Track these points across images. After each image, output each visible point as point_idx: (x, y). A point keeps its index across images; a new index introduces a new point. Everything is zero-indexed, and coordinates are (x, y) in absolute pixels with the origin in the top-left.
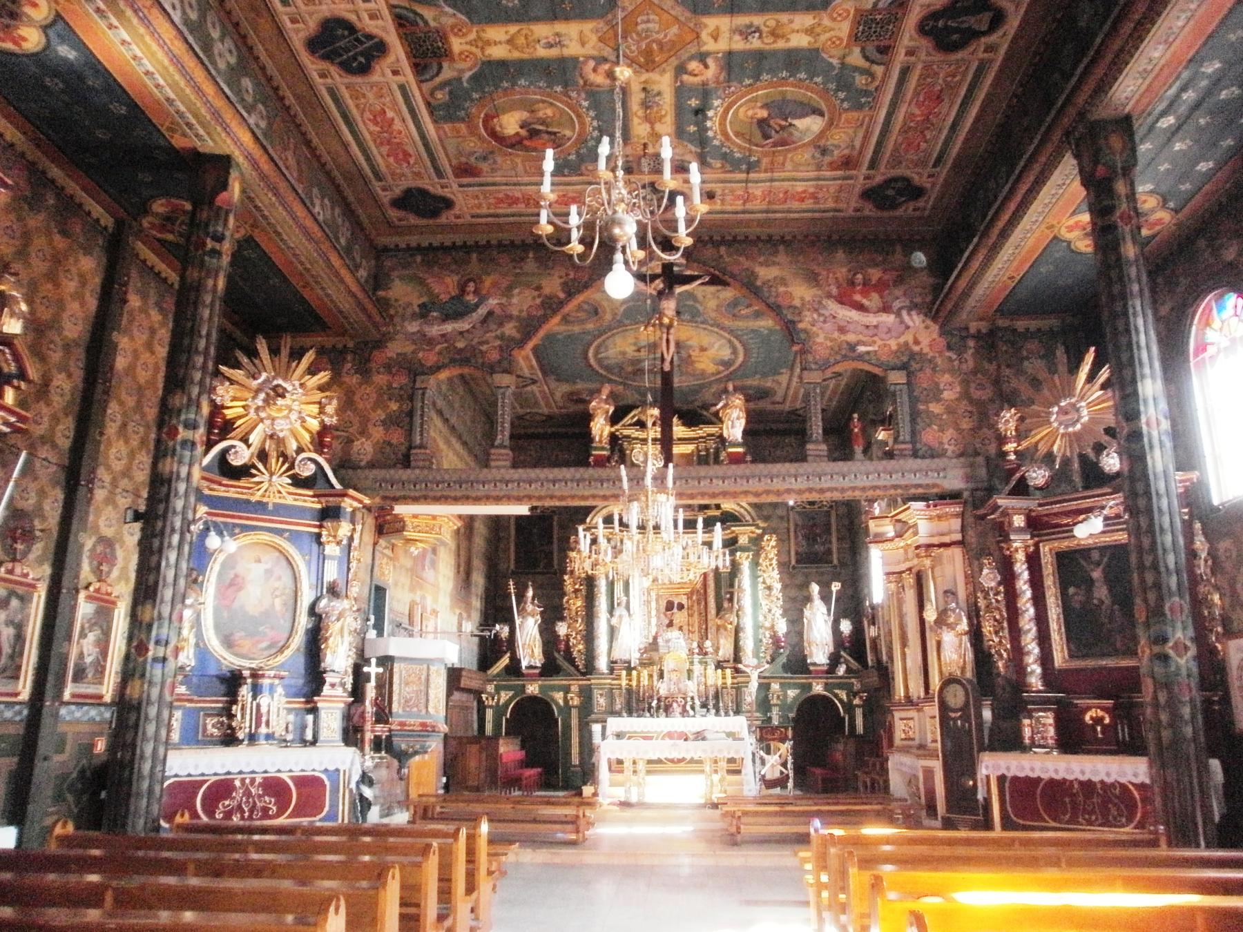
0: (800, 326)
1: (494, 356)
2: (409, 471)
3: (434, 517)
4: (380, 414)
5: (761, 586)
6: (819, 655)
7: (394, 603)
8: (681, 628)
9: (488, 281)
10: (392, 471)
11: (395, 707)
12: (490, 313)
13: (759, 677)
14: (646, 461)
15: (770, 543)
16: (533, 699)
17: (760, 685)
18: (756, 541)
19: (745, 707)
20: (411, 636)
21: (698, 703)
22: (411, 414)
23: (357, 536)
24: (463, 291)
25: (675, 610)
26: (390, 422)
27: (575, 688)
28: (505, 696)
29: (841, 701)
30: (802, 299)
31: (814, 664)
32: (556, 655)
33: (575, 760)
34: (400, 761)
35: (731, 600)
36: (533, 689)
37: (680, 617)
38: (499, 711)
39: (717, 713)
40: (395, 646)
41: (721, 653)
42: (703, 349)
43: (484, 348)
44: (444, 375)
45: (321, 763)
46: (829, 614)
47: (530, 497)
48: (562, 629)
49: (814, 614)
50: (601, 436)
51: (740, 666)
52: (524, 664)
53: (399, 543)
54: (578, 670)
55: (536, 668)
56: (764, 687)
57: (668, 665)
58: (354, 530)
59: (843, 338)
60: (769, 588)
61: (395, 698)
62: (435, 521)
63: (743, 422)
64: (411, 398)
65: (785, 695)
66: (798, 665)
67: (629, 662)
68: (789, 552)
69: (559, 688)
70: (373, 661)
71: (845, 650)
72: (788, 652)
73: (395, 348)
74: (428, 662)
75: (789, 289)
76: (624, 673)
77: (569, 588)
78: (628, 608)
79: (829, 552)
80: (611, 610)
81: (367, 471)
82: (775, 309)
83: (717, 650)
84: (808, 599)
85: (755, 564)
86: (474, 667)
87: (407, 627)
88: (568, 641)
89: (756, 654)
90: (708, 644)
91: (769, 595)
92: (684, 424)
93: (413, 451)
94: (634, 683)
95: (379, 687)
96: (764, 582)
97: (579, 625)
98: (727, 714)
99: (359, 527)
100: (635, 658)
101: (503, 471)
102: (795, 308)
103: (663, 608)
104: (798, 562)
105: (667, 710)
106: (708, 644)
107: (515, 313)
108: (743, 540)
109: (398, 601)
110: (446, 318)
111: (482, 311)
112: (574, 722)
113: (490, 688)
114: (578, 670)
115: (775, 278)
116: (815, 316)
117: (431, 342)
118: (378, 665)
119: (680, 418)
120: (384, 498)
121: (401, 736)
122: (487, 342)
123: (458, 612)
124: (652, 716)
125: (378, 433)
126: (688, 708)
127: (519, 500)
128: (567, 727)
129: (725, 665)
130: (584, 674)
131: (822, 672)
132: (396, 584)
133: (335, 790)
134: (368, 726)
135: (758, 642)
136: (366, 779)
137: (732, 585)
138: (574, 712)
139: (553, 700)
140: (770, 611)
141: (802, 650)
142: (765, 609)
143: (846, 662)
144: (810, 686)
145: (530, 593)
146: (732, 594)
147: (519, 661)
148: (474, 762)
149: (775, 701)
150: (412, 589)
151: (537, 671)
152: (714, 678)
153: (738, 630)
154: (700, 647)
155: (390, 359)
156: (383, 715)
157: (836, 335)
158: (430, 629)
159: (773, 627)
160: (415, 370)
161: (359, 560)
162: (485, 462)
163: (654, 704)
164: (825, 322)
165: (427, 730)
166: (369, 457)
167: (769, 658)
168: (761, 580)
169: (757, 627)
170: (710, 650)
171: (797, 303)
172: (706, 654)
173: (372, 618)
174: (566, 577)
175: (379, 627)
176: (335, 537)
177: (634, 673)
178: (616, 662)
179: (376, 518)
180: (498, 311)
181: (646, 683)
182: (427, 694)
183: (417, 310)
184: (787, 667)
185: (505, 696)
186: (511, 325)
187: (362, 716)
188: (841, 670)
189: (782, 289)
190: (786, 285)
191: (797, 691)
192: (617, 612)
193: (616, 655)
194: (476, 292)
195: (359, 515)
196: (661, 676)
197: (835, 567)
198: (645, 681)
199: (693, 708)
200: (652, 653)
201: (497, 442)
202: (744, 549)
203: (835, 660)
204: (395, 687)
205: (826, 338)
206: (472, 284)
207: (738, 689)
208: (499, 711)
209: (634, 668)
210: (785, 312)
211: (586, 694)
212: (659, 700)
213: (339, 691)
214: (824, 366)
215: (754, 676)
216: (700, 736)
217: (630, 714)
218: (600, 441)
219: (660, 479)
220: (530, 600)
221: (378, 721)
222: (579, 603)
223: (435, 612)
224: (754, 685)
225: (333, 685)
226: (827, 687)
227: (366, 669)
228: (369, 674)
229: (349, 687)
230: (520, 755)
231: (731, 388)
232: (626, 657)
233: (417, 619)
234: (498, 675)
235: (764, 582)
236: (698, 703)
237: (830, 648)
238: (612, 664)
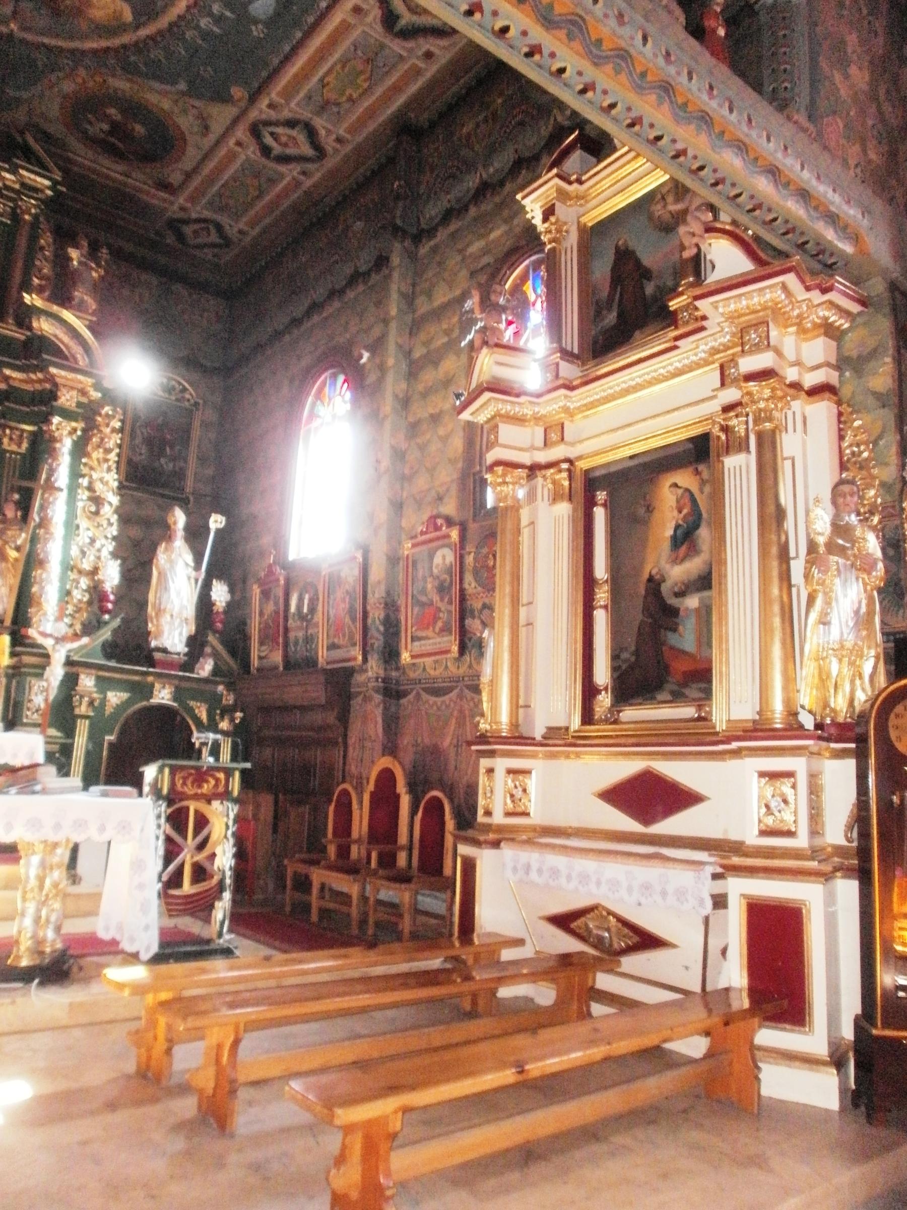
5: (83, 495)
6: (172, 632)
19: (29, 716)
31: (165, 651)
35: (25, 506)
46: (197, 567)
49: (171, 562)
56: (70, 681)
60: (97, 501)
65: (104, 700)
66: (131, 647)
71: (215, 632)
72: (117, 622)
79: (180, 475)
84: (167, 533)
85: (80, 450)
91: (97, 513)
108: (67, 399)
131: (171, 665)
140: (93, 541)
143: (215, 655)
144: (147, 691)
149: (83, 709)
153: (32, 562)
159: (95, 571)
168: (85, 482)
169: (68, 567)
184: (111, 650)
188: (206, 668)
191: (125, 696)
202: (67, 415)
224: (56, 673)
226: (178, 695)
235: (90, 488)
237: (191, 628)
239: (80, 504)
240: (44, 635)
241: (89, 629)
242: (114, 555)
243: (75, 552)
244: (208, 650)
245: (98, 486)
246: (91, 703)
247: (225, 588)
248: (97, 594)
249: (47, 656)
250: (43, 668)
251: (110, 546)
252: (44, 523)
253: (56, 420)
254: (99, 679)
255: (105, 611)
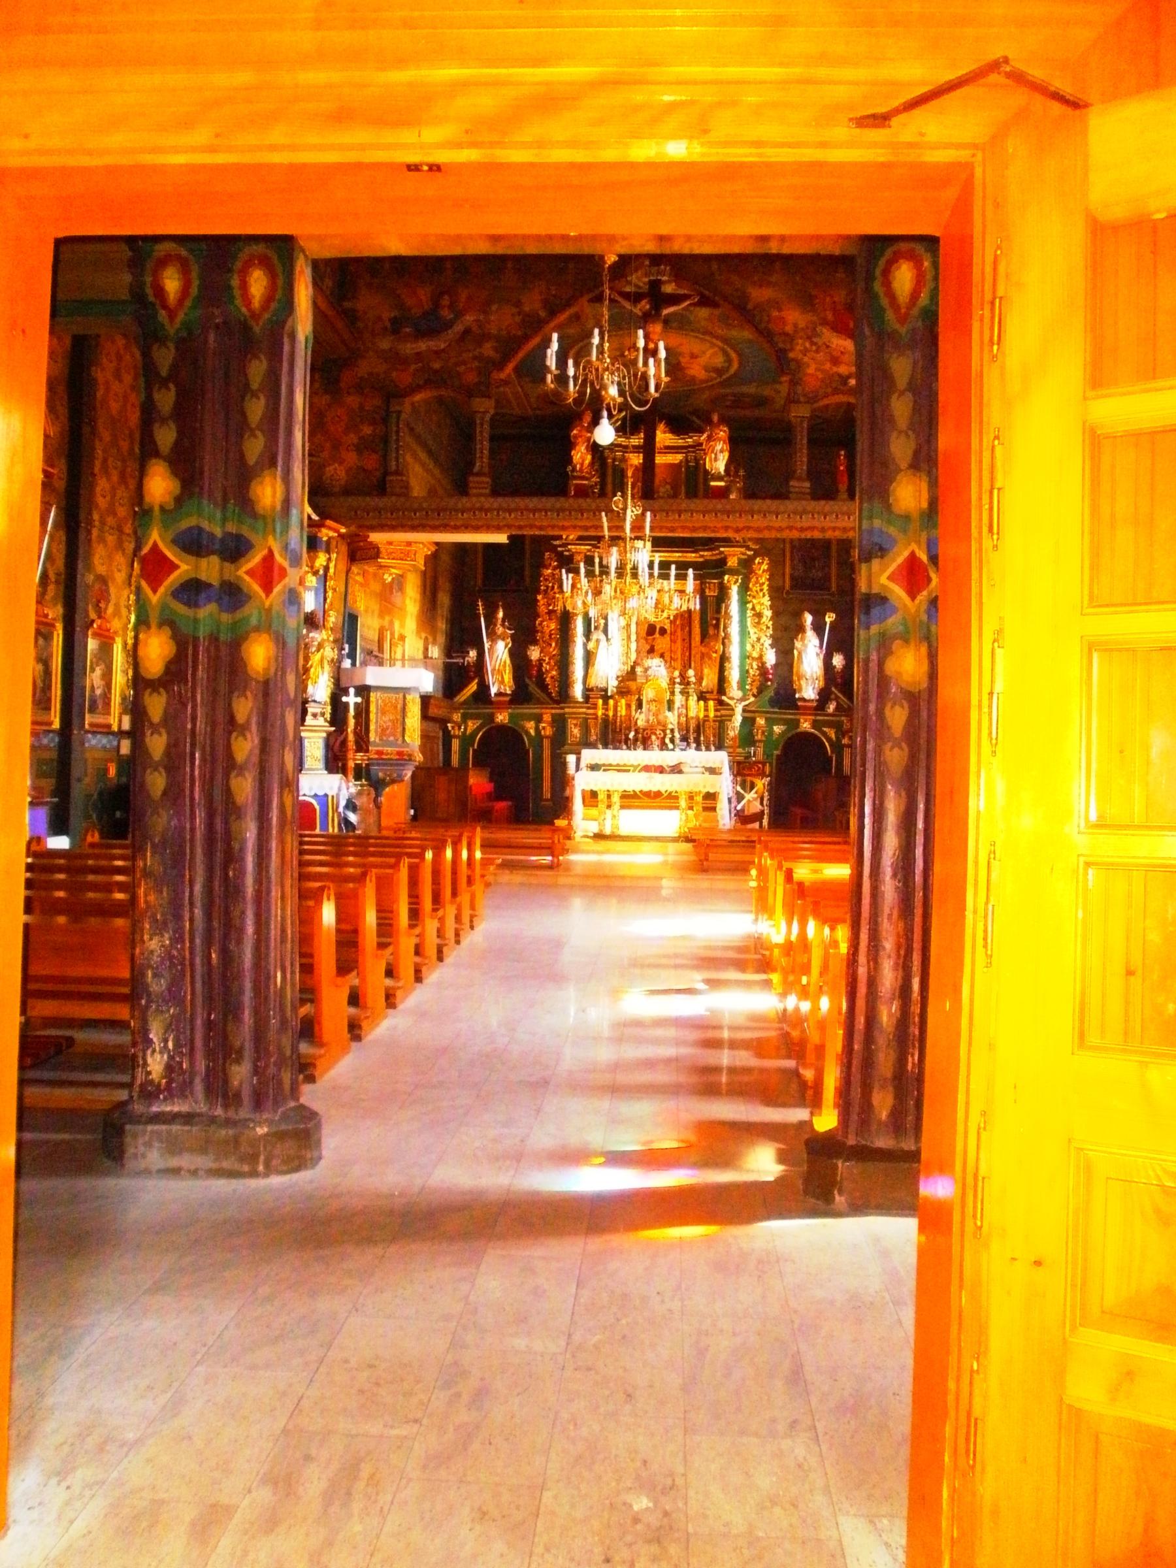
0: (791, 355)
1: (471, 378)
2: (385, 499)
3: (409, 544)
4: (353, 438)
5: (749, 613)
7: (366, 630)
8: (662, 656)
9: (463, 295)
10: (368, 499)
11: (373, 737)
12: (467, 331)
13: (744, 711)
14: (625, 509)
15: (762, 566)
16: (502, 728)
17: (745, 719)
18: (747, 566)
19: (728, 742)
20: (381, 664)
21: (677, 735)
22: (385, 440)
23: (332, 565)
24: (437, 305)
25: (657, 635)
26: (362, 447)
27: (547, 717)
28: (472, 725)
29: (829, 739)
30: (795, 325)
31: (803, 700)
32: (527, 680)
33: (547, 794)
34: (376, 790)
35: (717, 626)
36: (502, 717)
37: (662, 643)
38: (466, 741)
39: (698, 748)
40: (373, 676)
41: (704, 683)
42: (693, 356)
43: (462, 369)
44: (418, 397)
45: (311, 789)
46: (821, 647)
47: (509, 527)
48: (534, 653)
49: (805, 646)
50: (582, 465)
51: (724, 698)
52: (494, 690)
53: (371, 569)
54: (552, 698)
55: (505, 695)
56: (749, 722)
57: (648, 694)
58: (329, 560)
59: (835, 369)
61: (372, 727)
62: (408, 549)
63: (727, 455)
64: (385, 421)
65: (771, 732)
67: (606, 690)
68: (784, 574)
69: (530, 717)
70: (352, 691)
73: (364, 368)
74: (405, 691)
75: (784, 314)
76: (600, 702)
77: (542, 609)
78: (605, 631)
79: (827, 578)
80: (588, 634)
81: (342, 499)
82: (767, 334)
83: (700, 679)
84: (801, 629)
85: (744, 589)
86: (440, 695)
87: (376, 657)
88: (541, 665)
89: (741, 685)
90: (691, 673)
91: (759, 623)
92: (673, 431)
93: (389, 478)
94: (611, 713)
95: (357, 716)
96: (753, 609)
97: (553, 649)
98: (708, 749)
99: (334, 556)
100: (612, 685)
101: (483, 499)
102: (787, 335)
103: (643, 633)
104: (792, 588)
105: (646, 743)
106: (691, 673)
107: (494, 331)
108: (732, 562)
109: (369, 628)
110: (420, 334)
111: (459, 328)
112: (547, 753)
113: (457, 717)
114: (552, 698)
115: (769, 301)
116: (807, 345)
117: (404, 361)
118: (357, 695)
119: (667, 424)
120: (360, 527)
121: (378, 765)
122: (464, 363)
123: (423, 635)
124: (629, 748)
125: (351, 458)
126: (667, 741)
127: (498, 529)
128: (539, 758)
129: (708, 696)
130: (558, 702)
132: (366, 611)
133: (325, 814)
134: (350, 755)
135: (744, 673)
136: (351, 805)
137: (718, 611)
138: (546, 743)
139: (523, 727)
140: (759, 639)
141: (791, 682)
142: (754, 637)
143: (837, 699)
145: (501, 614)
146: (718, 620)
147: (488, 688)
148: (442, 792)
150: (381, 615)
151: (507, 699)
152: (696, 709)
154: (683, 676)
155: (361, 378)
156: (362, 743)
157: (828, 366)
158: (399, 656)
159: (761, 657)
160: (392, 394)
161: (334, 590)
162: (462, 488)
163: (632, 735)
164: (817, 351)
165: (403, 758)
166: (343, 482)
167: (755, 691)
168: (750, 606)
169: (744, 656)
170: (693, 679)
171: (789, 329)
172: (688, 683)
173: (347, 646)
174: (539, 597)
175: (352, 655)
176: (312, 567)
177: (611, 702)
178: (591, 690)
179: (349, 544)
180: (475, 328)
181: (624, 713)
182: (404, 723)
183: (388, 324)
184: (773, 702)
185: (472, 725)
186: (488, 345)
187: (344, 743)
188: (831, 707)
189: (775, 313)
190: (780, 310)
191: (783, 728)
192: (594, 637)
193: (592, 682)
194: (451, 307)
195: (334, 543)
196: (640, 705)
197: (833, 595)
198: (622, 711)
199: (672, 741)
200: (629, 682)
201: (476, 469)
202: (732, 572)
203: (824, 695)
204: (372, 716)
205: (817, 369)
206: (446, 297)
207: (722, 723)
208: (466, 741)
209: (612, 697)
210: (775, 339)
211: (560, 723)
212: (637, 732)
213: (321, 721)
214: (812, 399)
215: (739, 710)
216: (677, 769)
217: (606, 746)
218: (581, 470)
219: (638, 526)
220: (500, 621)
221: (359, 750)
222: (553, 626)
223: (402, 638)
224: (738, 719)
225: (315, 715)
226: (815, 724)
227: (344, 699)
228: (347, 705)
229: (328, 716)
230: (490, 787)
231: (715, 418)
232: (602, 685)
233: (387, 646)
234: (465, 703)
235: (753, 609)
236: (677, 735)
237: (821, 683)
238: (588, 691)
239: (749, 620)
240: (732, 699)
241: (761, 690)
242: (772, 646)
243: (749, 647)
244: (833, 696)
245: (758, 608)
246: (763, 733)
247: (841, 657)
248: (762, 669)
249: (733, 710)
250: (731, 716)
251: (770, 642)
252: (727, 636)
253: (726, 577)
254: (767, 719)
255: (768, 680)
